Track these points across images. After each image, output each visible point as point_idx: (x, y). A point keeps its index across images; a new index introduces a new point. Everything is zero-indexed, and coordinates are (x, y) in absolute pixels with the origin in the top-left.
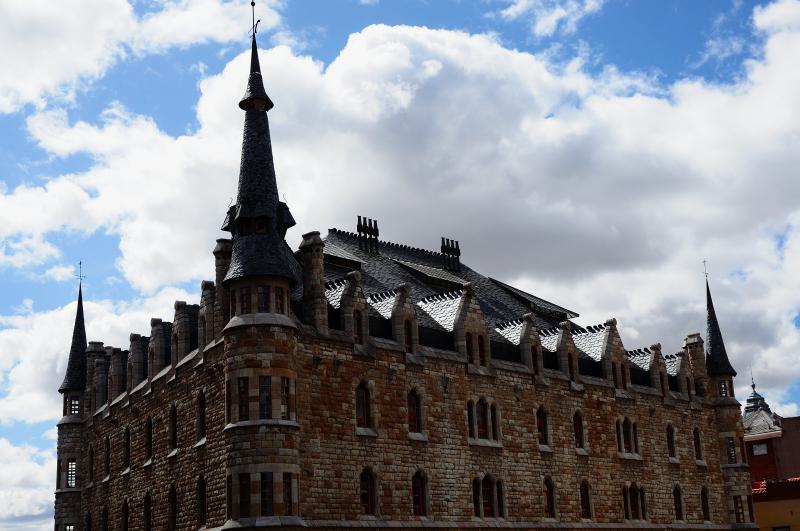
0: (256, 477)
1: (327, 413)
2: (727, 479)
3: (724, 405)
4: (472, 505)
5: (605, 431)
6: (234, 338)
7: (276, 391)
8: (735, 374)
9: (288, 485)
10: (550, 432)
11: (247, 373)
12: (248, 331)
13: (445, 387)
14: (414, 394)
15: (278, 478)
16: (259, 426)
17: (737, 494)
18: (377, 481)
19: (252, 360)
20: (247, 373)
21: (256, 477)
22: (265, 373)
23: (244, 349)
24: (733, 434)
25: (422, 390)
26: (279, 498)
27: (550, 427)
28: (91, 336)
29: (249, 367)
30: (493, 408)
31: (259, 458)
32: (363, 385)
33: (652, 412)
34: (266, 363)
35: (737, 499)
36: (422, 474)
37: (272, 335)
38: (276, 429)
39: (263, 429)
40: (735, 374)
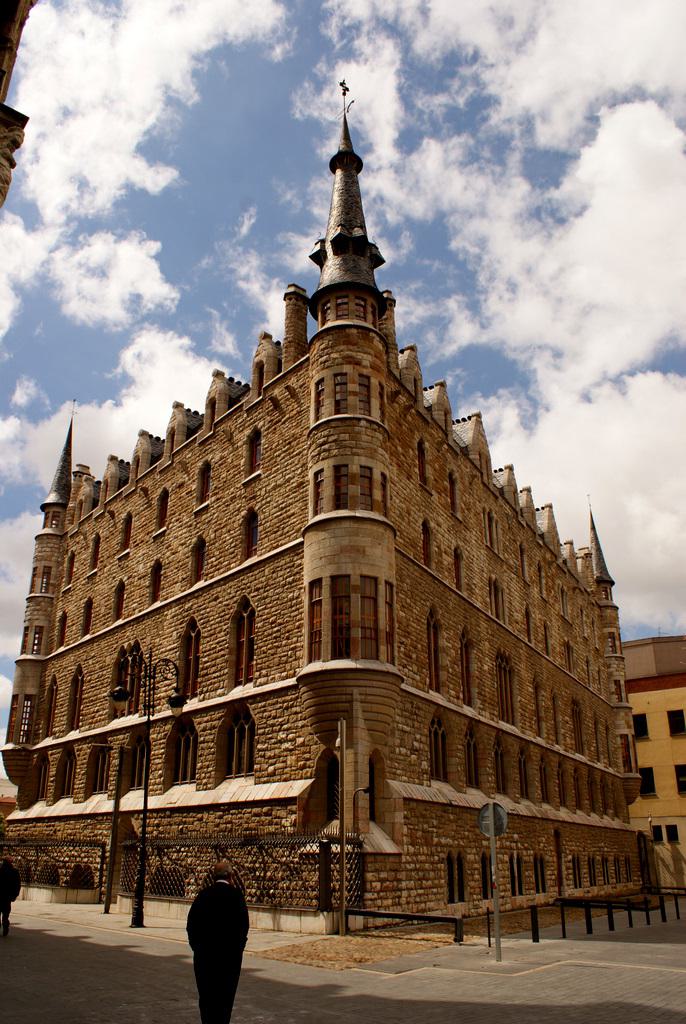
0: (354, 469)
1: (399, 449)
2: (609, 666)
3: (607, 607)
4: (488, 599)
5: (553, 588)
6: (330, 337)
7: (375, 392)
8: (612, 583)
9: (384, 487)
10: (526, 568)
11: (347, 368)
12: (347, 330)
13: (470, 484)
14: (451, 475)
15: (377, 476)
16: (359, 419)
17: (617, 678)
18: (432, 537)
19: (351, 357)
20: (347, 368)
21: (354, 469)
22: (365, 372)
23: (342, 347)
24: (613, 630)
25: (456, 475)
26: (377, 495)
27: (526, 563)
28: (76, 459)
29: (350, 363)
30: (497, 521)
31: (359, 451)
32: (421, 444)
33: (574, 589)
34: (366, 363)
35: (617, 683)
36: (459, 551)
37: (371, 340)
38: (376, 427)
39: (363, 423)
40: (612, 583)
